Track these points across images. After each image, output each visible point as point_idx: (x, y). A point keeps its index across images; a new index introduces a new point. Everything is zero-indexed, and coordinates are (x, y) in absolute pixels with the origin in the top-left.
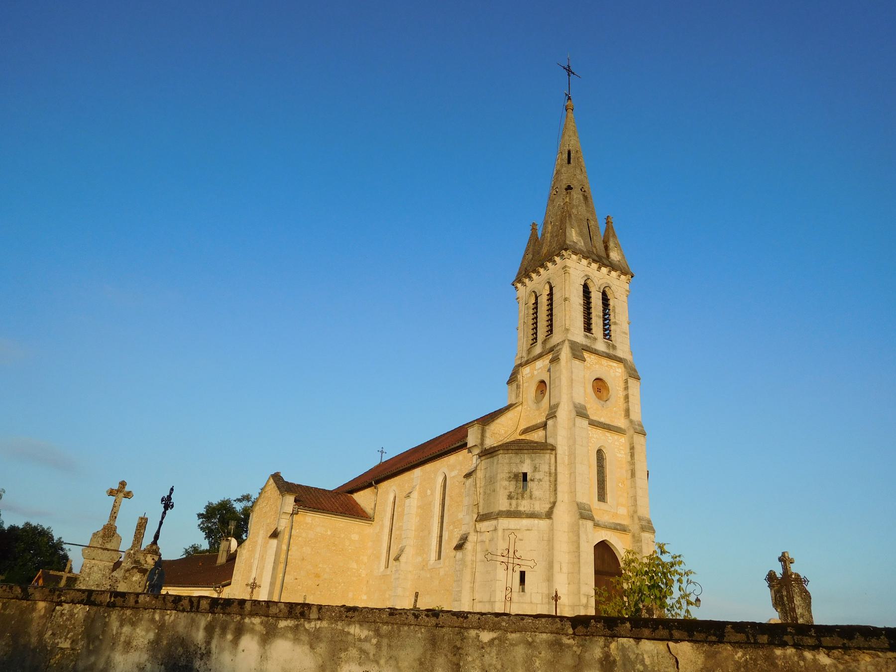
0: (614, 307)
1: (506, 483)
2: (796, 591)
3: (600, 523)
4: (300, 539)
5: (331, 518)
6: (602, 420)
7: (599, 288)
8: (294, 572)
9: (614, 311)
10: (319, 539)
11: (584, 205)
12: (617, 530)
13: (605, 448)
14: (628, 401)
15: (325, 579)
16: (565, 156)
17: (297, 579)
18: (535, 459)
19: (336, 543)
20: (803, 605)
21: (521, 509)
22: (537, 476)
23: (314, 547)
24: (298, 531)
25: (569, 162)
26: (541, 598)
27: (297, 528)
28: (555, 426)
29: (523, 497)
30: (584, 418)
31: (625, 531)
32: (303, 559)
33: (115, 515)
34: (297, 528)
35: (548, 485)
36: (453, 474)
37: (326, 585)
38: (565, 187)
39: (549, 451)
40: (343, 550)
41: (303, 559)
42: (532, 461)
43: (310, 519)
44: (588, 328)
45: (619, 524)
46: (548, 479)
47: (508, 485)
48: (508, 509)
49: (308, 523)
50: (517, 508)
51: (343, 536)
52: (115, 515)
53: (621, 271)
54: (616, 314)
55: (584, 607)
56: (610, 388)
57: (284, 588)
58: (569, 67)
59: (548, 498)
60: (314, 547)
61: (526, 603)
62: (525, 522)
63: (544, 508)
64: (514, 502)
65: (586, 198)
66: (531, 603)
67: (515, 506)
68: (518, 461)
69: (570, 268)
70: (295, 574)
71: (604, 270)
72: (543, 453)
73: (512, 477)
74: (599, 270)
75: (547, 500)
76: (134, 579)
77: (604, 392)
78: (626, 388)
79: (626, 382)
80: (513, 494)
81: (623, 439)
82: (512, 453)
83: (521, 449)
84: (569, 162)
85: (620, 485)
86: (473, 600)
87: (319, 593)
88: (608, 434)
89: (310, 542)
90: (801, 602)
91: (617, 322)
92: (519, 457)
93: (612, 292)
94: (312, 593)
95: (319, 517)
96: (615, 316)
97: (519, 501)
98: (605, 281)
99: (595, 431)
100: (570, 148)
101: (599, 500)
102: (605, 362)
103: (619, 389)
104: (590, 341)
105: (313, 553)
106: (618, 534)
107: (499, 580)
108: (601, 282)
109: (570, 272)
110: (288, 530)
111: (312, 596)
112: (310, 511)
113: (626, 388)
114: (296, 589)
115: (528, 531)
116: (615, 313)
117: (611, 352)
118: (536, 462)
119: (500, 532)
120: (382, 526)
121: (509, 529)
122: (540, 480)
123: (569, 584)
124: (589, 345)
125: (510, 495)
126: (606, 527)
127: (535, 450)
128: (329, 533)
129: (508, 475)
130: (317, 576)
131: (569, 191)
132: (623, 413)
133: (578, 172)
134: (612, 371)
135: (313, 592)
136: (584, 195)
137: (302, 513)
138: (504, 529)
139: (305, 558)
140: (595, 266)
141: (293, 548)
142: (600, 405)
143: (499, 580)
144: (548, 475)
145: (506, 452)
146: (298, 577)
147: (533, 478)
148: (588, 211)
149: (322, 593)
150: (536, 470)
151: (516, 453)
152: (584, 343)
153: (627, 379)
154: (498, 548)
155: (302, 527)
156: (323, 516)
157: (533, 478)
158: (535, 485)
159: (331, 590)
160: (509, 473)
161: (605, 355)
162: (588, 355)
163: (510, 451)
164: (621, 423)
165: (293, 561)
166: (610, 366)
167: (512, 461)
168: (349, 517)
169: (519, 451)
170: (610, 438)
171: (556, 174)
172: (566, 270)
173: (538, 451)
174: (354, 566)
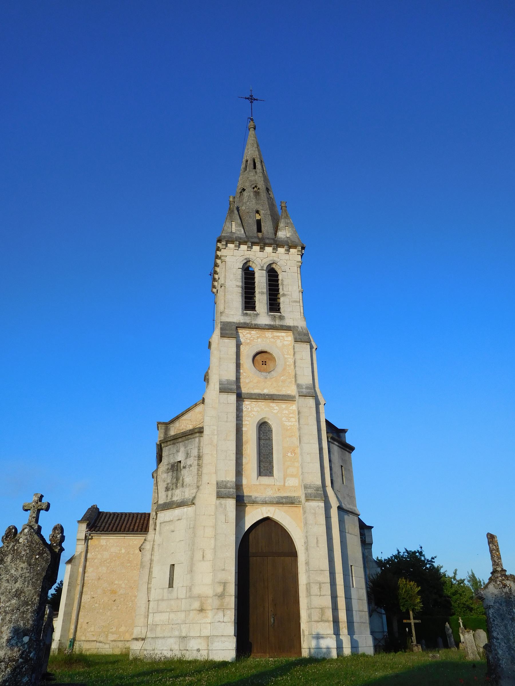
0: (282, 280)
1: (165, 475)
2: (23, 553)
3: (258, 499)
4: (96, 561)
5: (124, 537)
6: (266, 391)
7: (263, 267)
8: (91, 591)
10: (114, 559)
12: (282, 503)
13: (269, 419)
15: (122, 594)
17: (93, 598)
18: (188, 445)
19: (130, 559)
20: (28, 575)
21: (175, 499)
22: (189, 462)
23: (109, 567)
24: (93, 553)
26: (185, 592)
27: (93, 551)
29: (176, 487)
30: (229, 394)
31: (292, 503)
32: (99, 579)
34: (93, 551)
35: (196, 470)
37: (122, 599)
39: (197, 435)
41: (99, 579)
42: (185, 448)
43: (105, 542)
45: (283, 498)
46: (197, 463)
47: (166, 476)
48: (165, 501)
49: (103, 546)
50: (172, 499)
53: (288, 245)
54: (284, 286)
55: (219, 597)
56: (276, 358)
57: (81, 607)
59: (195, 482)
60: (109, 567)
61: (173, 599)
62: (177, 512)
63: (192, 494)
64: (170, 493)
66: (177, 598)
67: (171, 497)
68: (175, 451)
70: (92, 593)
72: (194, 438)
73: (170, 468)
74: (262, 250)
75: (195, 485)
77: (270, 364)
80: (169, 485)
82: (170, 445)
83: (176, 439)
85: (289, 454)
86: (149, 601)
87: (115, 608)
88: (272, 404)
90: (25, 571)
92: (176, 447)
93: (279, 267)
94: (109, 609)
95: (104, 538)
96: (283, 289)
97: (174, 491)
98: (271, 258)
99: (256, 405)
101: (260, 473)
102: (269, 334)
103: (289, 356)
104: (249, 318)
105: (108, 572)
106: (286, 508)
107: (154, 578)
110: (83, 555)
111: (109, 612)
112: (102, 534)
114: (93, 607)
117: (278, 323)
118: (188, 448)
121: (164, 522)
122: (191, 466)
124: (248, 322)
125: (167, 487)
126: (265, 503)
127: (187, 437)
128: (123, 551)
129: (166, 468)
130: (114, 592)
134: (278, 341)
135: (110, 608)
137: (96, 537)
139: (101, 578)
141: (89, 569)
142: (262, 377)
143: (154, 578)
144: (197, 458)
145: (166, 445)
146: (94, 596)
147: (185, 466)
149: (119, 608)
150: (188, 456)
151: (174, 444)
152: (242, 321)
156: (116, 537)
157: (185, 466)
158: (186, 472)
159: (128, 603)
160: (168, 464)
161: (267, 327)
162: (248, 331)
163: (169, 443)
164: (292, 391)
165: (90, 581)
166: (276, 336)
167: (171, 452)
168: (140, 534)
169: (175, 441)
173: (189, 436)
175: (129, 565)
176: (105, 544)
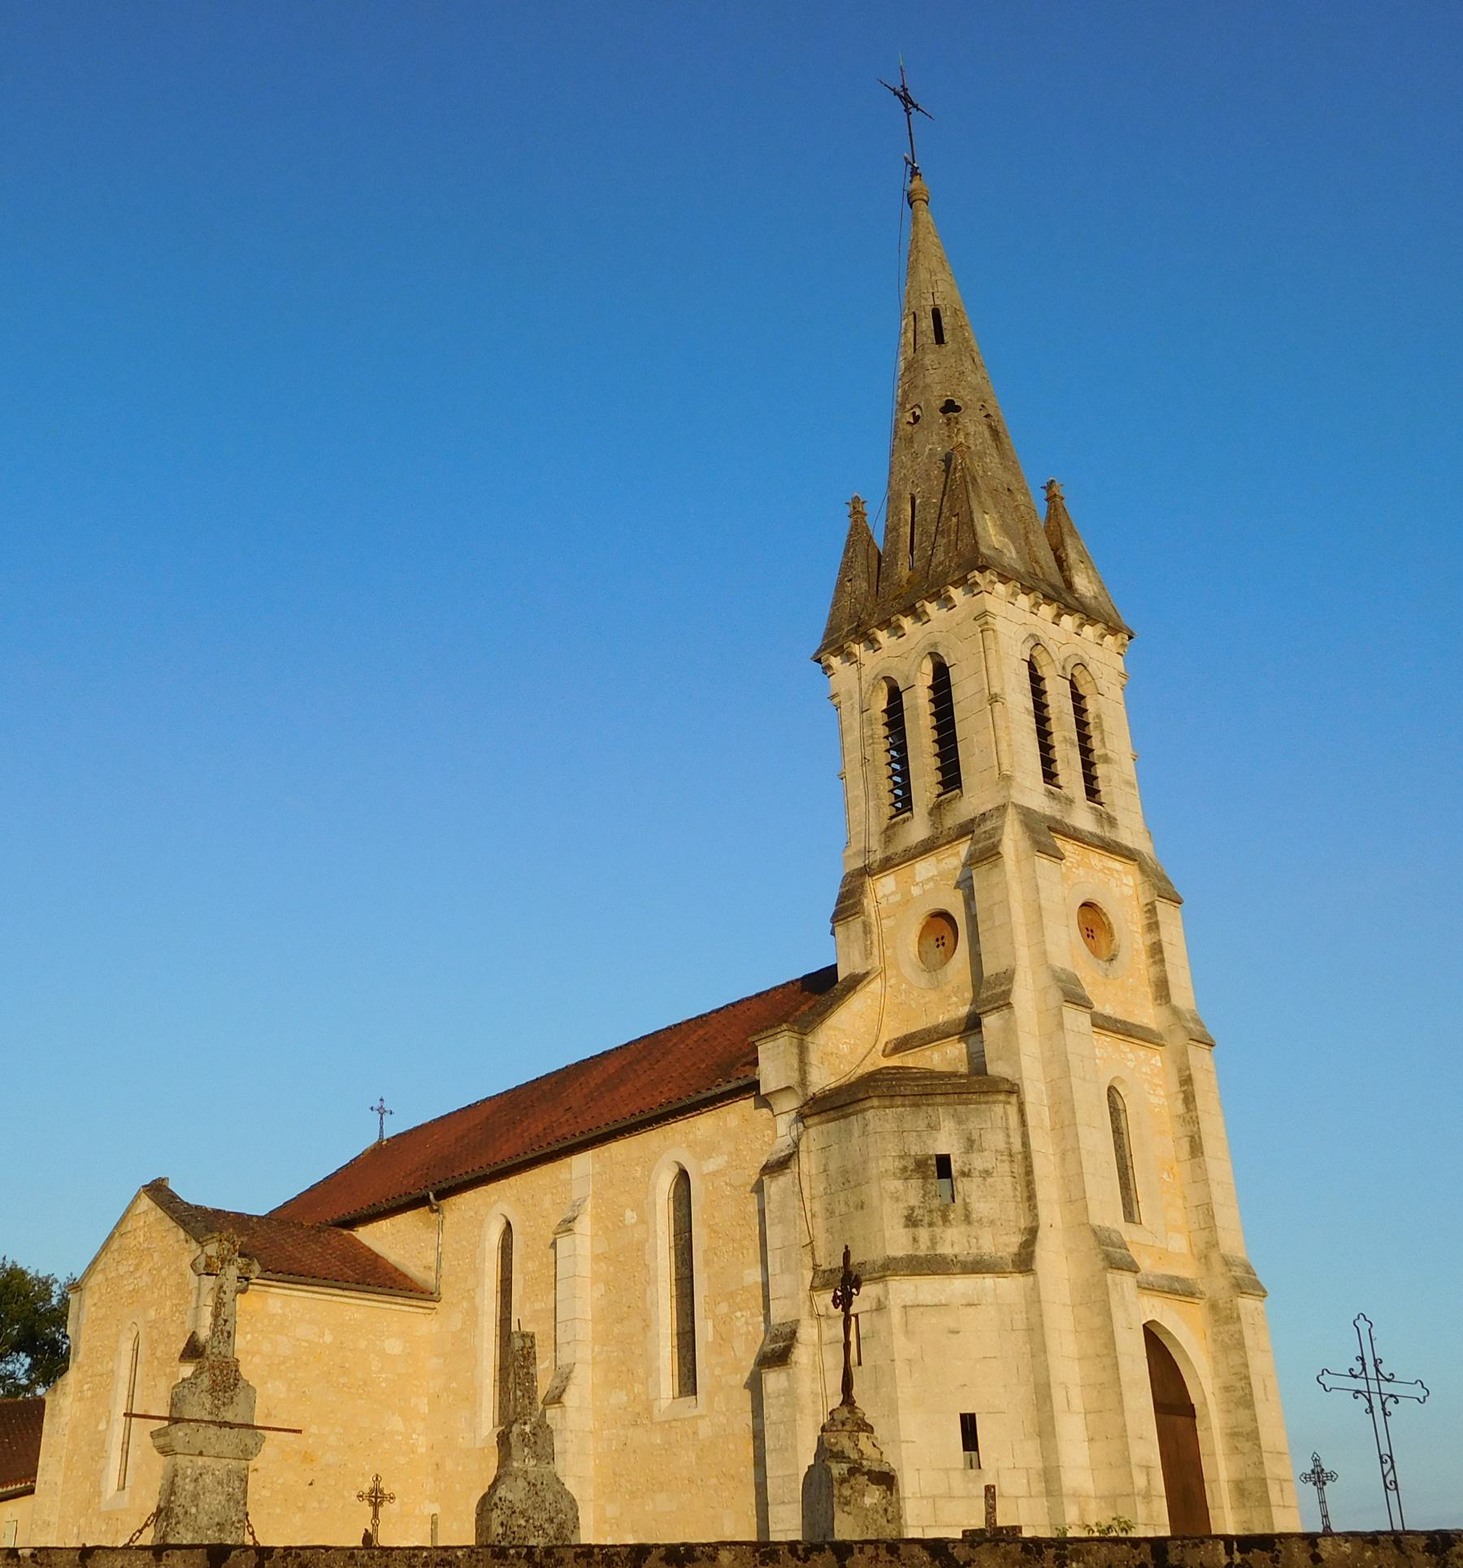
0: (1098, 716)
1: (895, 1185)
4: (257, 1360)
9: (1099, 726)
10: (304, 1358)
11: (994, 452)
12: (1176, 1293)
13: (1123, 1082)
14: (1162, 961)
16: (927, 324)
21: (946, 1250)
22: (979, 1162)
24: (249, 1337)
25: (940, 339)
26: (1025, 1481)
28: (1009, 1030)
29: (945, 1219)
30: (1080, 1008)
31: (1192, 1295)
33: (227, 1328)
34: (248, 1329)
35: (1010, 1186)
36: (711, 1166)
38: (941, 403)
39: (1002, 1097)
40: (365, 1383)
42: (960, 1123)
43: (279, 1304)
44: (1049, 776)
45: (1177, 1279)
50: (935, 1250)
51: (362, 1344)
52: (227, 1328)
54: (1106, 734)
55: (1144, 1498)
56: (1115, 927)
58: (905, 90)
62: (960, 1285)
64: (923, 1233)
65: (995, 433)
67: (929, 1244)
69: (994, 616)
71: (1068, 621)
72: (987, 1103)
73: (911, 1167)
76: (868, 1501)
78: (1153, 926)
79: (1151, 910)
81: (1158, 1058)
82: (903, 1106)
83: (927, 1095)
84: (940, 339)
85: (1165, 1176)
87: (316, 1504)
89: (283, 1367)
91: (1110, 754)
92: (922, 1114)
93: (1089, 679)
94: (298, 1508)
96: (1103, 740)
97: (938, 1230)
99: (1097, 1040)
100: (938, 302)
107: (907, 1442)
108: (1066, 651)
109: (997, 628)
113: (1153, 926)
114: (257, 1497)
115: (970, 1310)
116: (1102, 732)
117: (1107, 833)
118: (971, 1126)
119: (896, 1316)
120: (473, 1313)
121: (918, 1305)
122: (987, 1173)
123: (1091, 1440)
127: (965, 1096)
128: (328, 1339)
129: (898, 1164)
131: (950, 414)
132: (1149, 991)
133: (968, 364)
134: (1113, 883)
135: (300, 1504)
136: (990, 426)
138: (905, 1307)
139: (273, 1413)
140: (1046, 611)
142: (1101, 973)
148: (1006, 468)
150: (972, 1146)
151: (917, 1105)
152: (1048, 812)
153: (1152, 903)
154: (896, 1357)
155: (259, 1325)
156: (310, 1295)
158: (974, 1187)
160: (901, 1157)
164: (1148, 1015)
166: (1109, 869)
167: (907, 1126)
170: (1130, 1056)
171: (907, 369)
172: (986, 623)
174: (397, 1423)
175: (343, 1380)
176: (280, 1311)
